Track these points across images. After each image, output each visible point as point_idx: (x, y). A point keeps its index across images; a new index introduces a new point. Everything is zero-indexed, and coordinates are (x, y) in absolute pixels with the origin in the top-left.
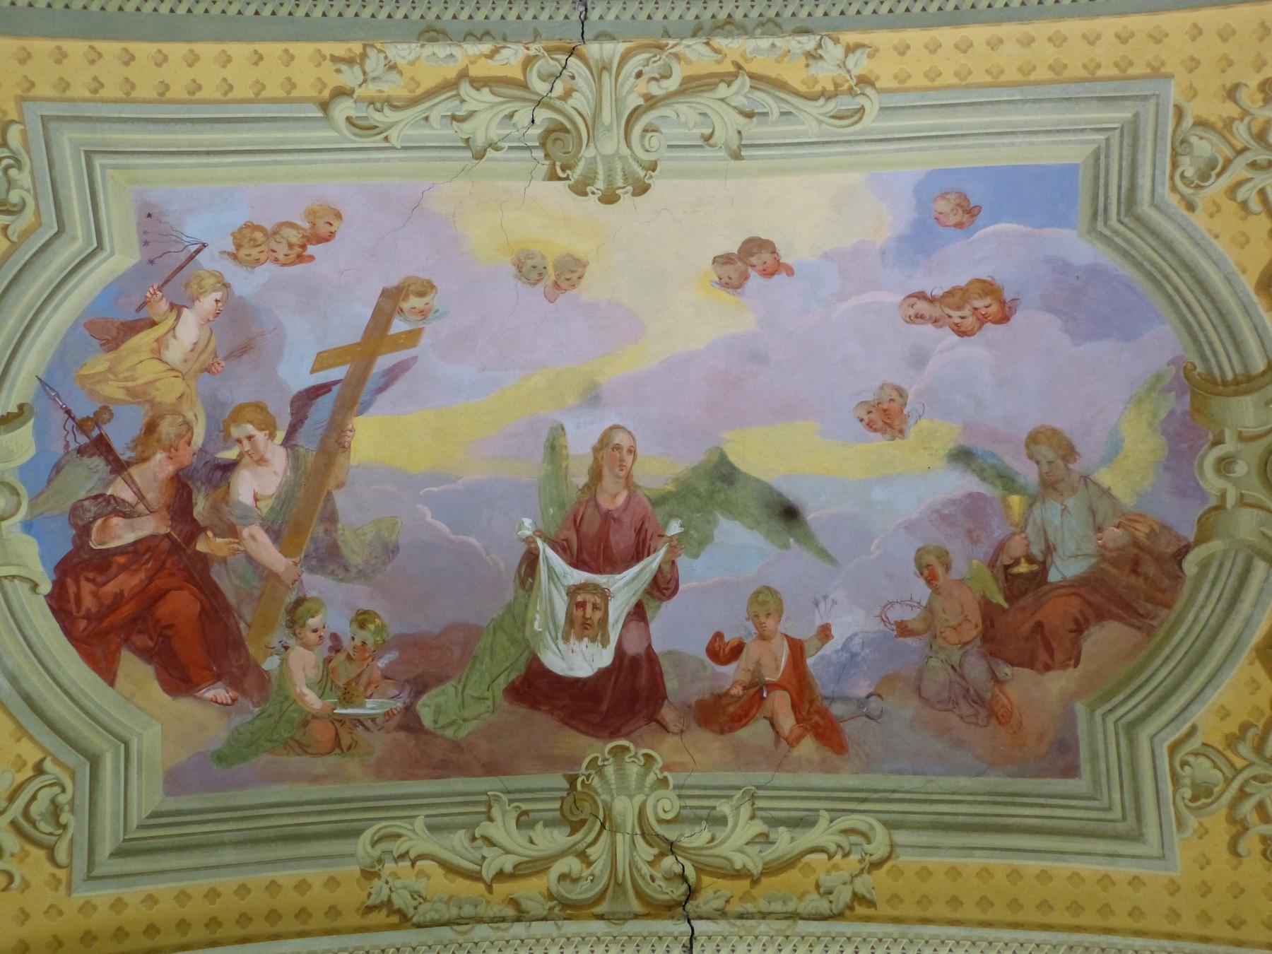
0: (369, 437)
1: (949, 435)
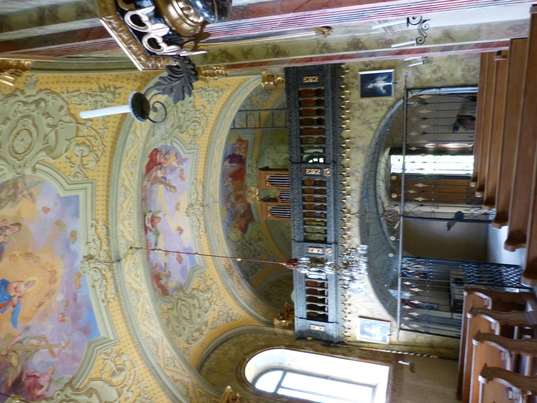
0: (161, 187)
1: (167, 262)
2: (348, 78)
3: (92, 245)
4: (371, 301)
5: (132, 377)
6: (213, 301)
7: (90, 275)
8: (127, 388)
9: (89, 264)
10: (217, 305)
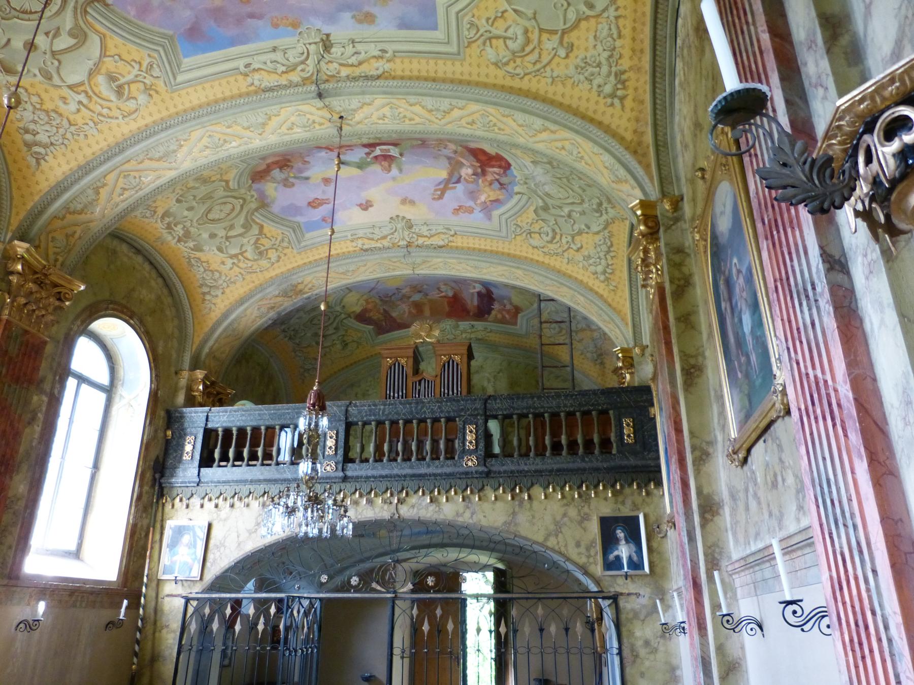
0: (444, 174)
1: (311, 181)
2: (632, 494)
3: (350, 50)
4: (239, 544)
5: (105, 111)
6: (239, 260)
7: (294, 45)
8: (85, 101)
9: (315, 43)
10: (231, 269)
